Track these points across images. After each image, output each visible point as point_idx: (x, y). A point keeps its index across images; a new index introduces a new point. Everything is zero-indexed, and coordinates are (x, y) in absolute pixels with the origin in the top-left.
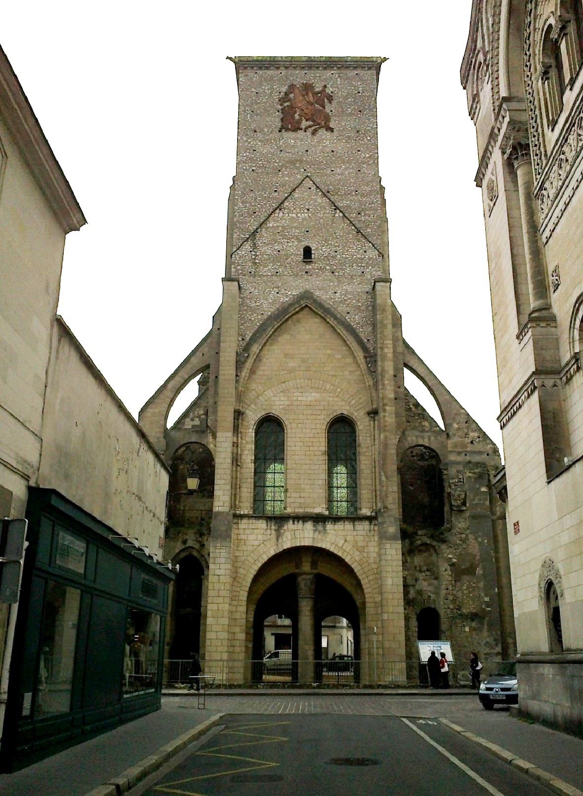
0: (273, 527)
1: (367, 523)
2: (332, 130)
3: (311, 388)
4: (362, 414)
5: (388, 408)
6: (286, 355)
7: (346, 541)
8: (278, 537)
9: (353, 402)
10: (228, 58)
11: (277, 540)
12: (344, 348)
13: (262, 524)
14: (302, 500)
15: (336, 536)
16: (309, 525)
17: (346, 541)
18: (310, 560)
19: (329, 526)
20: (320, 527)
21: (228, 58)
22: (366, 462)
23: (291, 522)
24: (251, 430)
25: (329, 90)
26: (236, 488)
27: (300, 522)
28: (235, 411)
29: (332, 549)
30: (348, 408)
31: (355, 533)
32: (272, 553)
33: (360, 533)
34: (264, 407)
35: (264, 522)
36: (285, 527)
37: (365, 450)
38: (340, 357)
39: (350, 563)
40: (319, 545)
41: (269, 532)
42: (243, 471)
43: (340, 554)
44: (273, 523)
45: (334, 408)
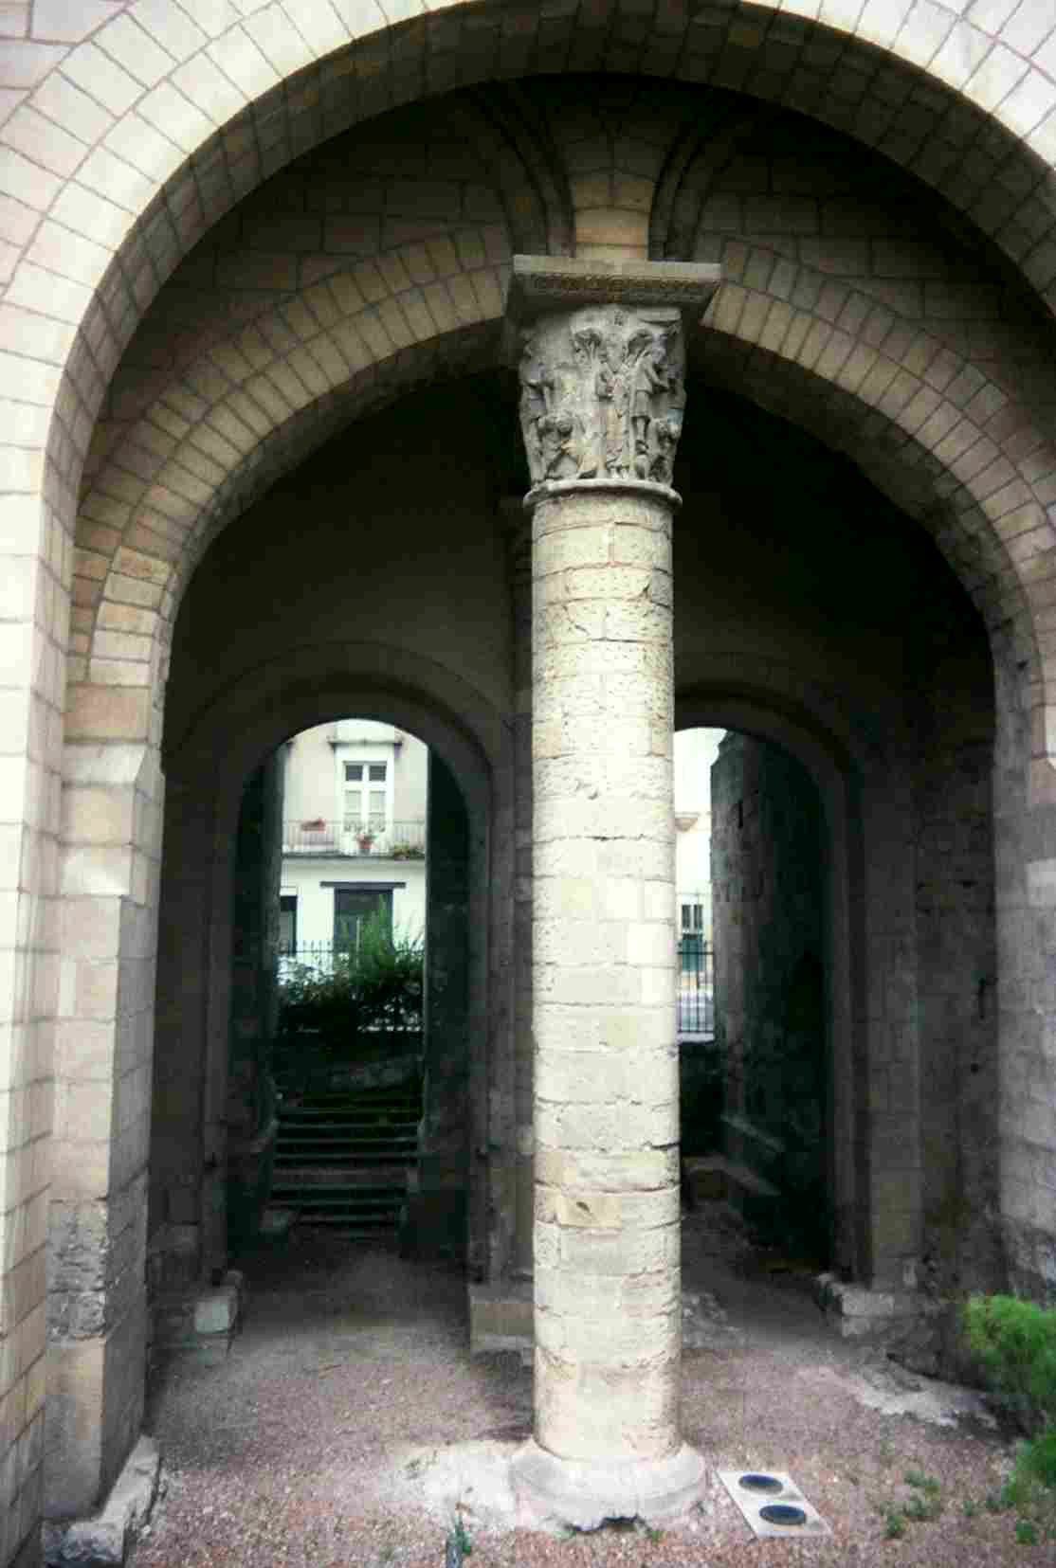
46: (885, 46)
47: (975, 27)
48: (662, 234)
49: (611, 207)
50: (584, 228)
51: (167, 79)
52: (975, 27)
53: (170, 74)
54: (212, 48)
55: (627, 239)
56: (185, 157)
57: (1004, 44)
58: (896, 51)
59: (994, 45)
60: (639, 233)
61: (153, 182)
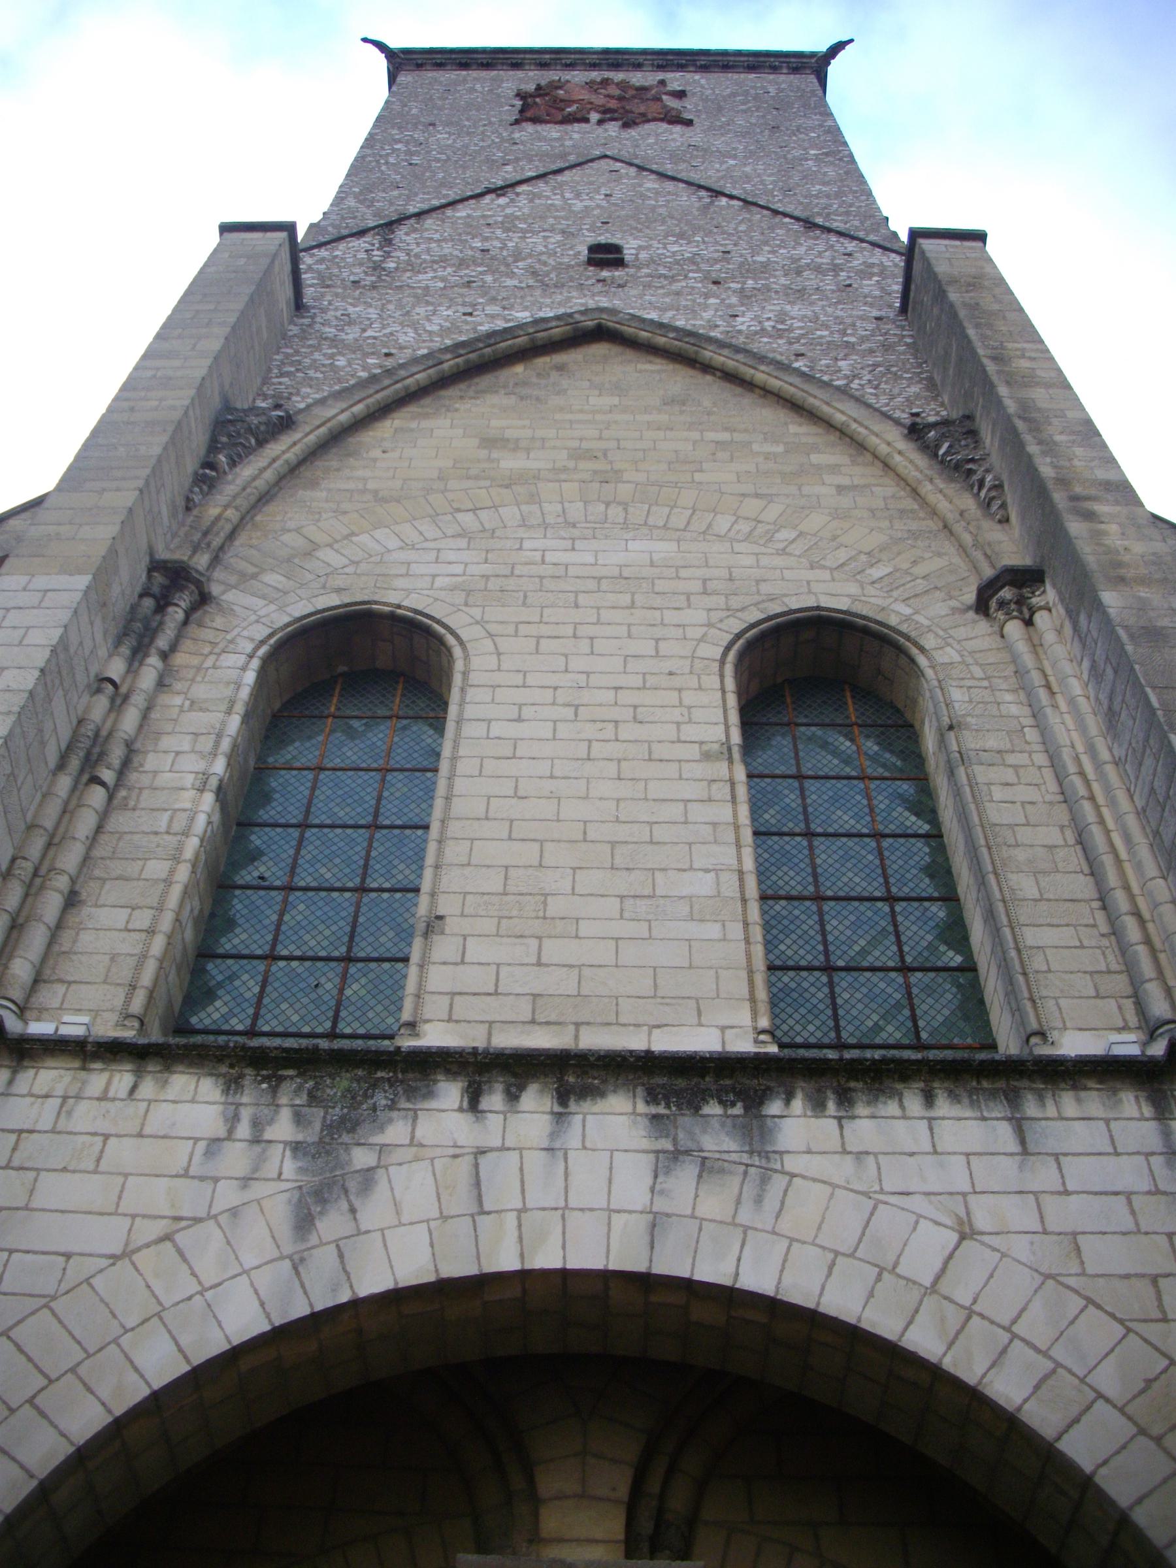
0: (283, 1128)
1: (1131, 1103)
2: (689, 123)
3: (625, 526)
4: (939, 608)
5: (1101, 508)
6: (490, 442)
7: (966, 1232)
8: (326, 1188)
9: (876, 572)
10: (365, 40)
11: (304, 1223)
12: (798, 429)
13: (191, 1103)
14: (557, 982)
15: (875, 1198)
16: (616, 1122)
17: (966, 1232)
18: (616, 1482)
19: (797, 1125)
20: (714, 1130)
21: (365, 40)
22: (1023, 793)
23: (450, 1092)
24: (233, 660)
25: (676, 86)
26: (34, 886)
27: (536, 1101)
28: (156, 566)
29: (843, 1300)
30: (853, 589)
31: (1045, 1176)
32: (241, 1318)
33: (1079, 1172)
34: (339, 582)
35: (209, 1088)
36: (396, 1131)
37: (992, 743)
38: (780, 449)
39: (1042, 1418)
40: (712, 1270)
41: (236, 1158)
42: (119, 821)
43: (924, 1341)
44: (290, 1095)
45: (765, 588)
46: (852, 1320)
47: (946, 1298)
48: (646, 1526)
49: (582, 1496)
50: (551, 1521)
51: (73, 1370)
52: (946, 1298)
53: (79, 1364)
54: (125, 1341)
55: (599, 1534)
56: (71, 1450)
57: (981, 1315)
58: (864, 1325)
59: (969, 1318)
60: (614, 1525)
61: (32, 1476)
